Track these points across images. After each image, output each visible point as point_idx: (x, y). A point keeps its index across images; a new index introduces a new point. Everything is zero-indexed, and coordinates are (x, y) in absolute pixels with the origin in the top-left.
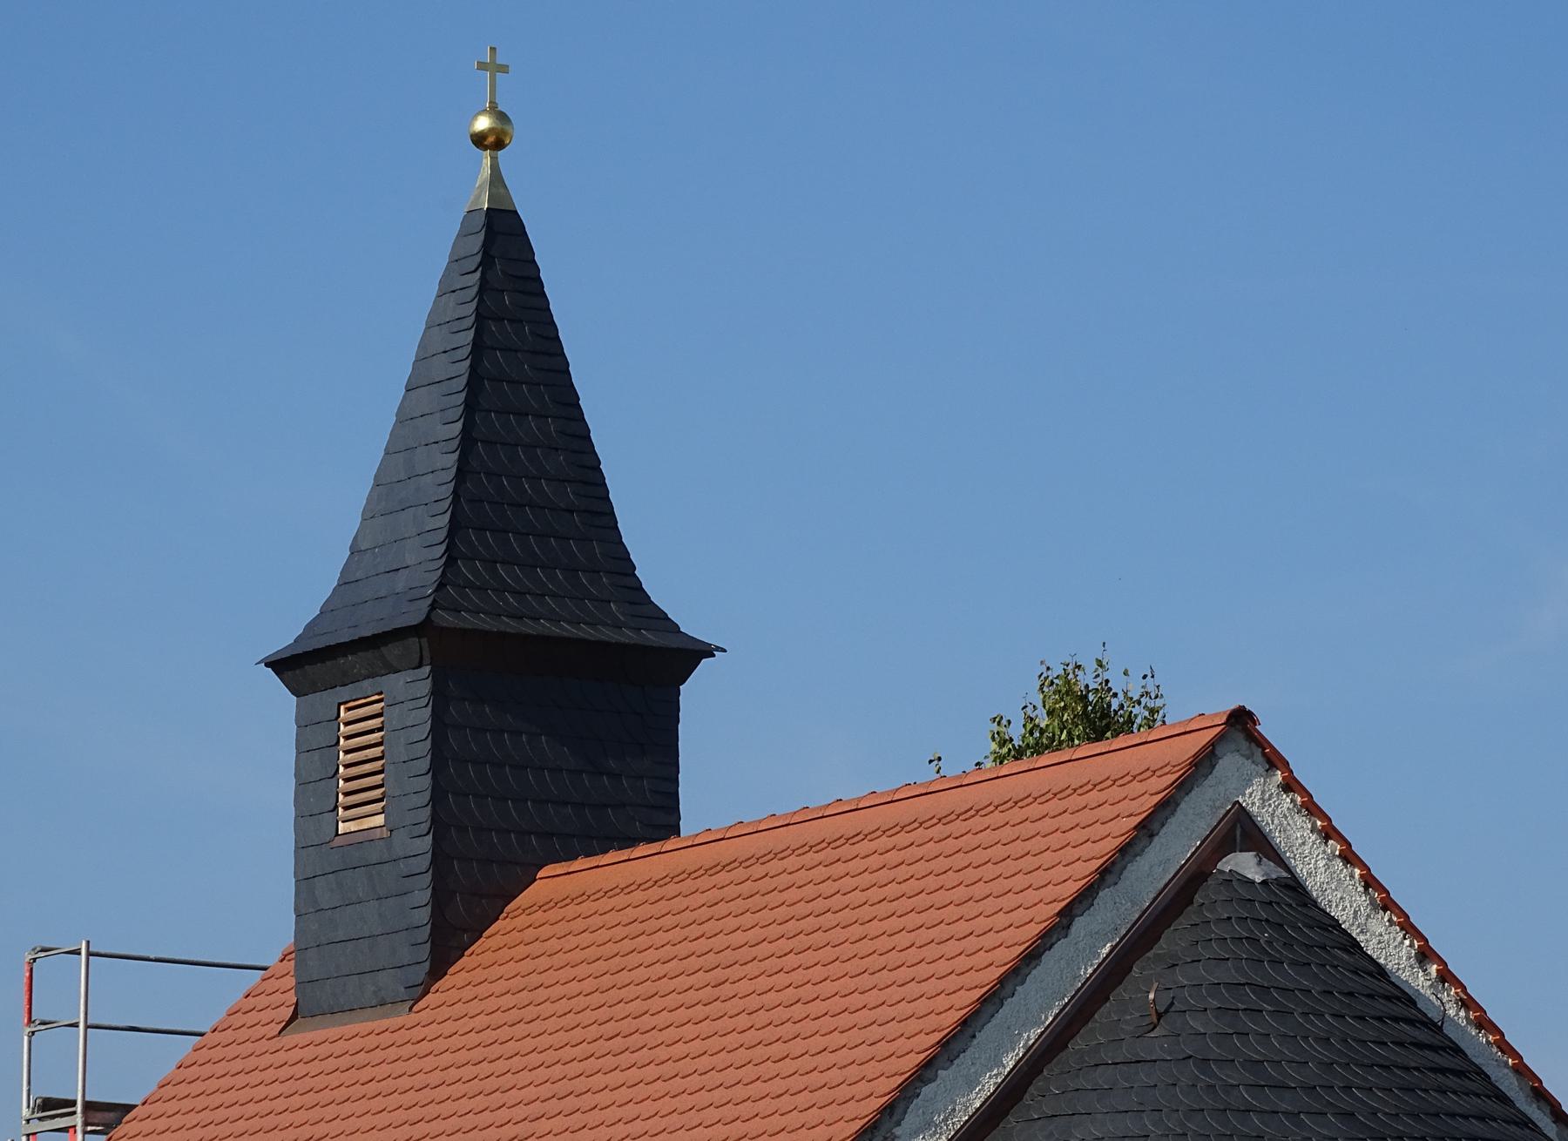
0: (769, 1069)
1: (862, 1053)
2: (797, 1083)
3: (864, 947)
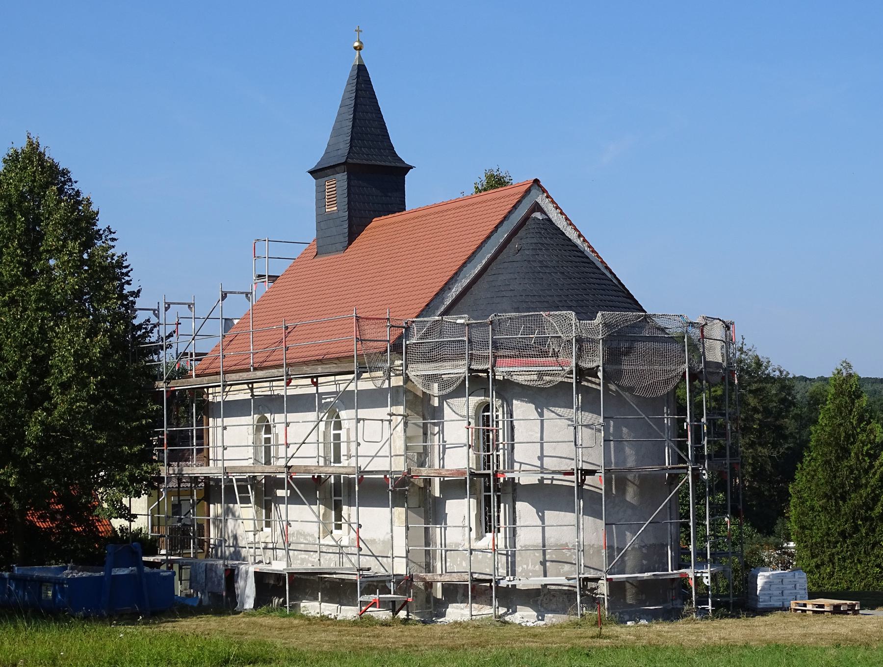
0: (427, 265)
1: (450, 260)
2: (434, 268)
3: (449, 236)
